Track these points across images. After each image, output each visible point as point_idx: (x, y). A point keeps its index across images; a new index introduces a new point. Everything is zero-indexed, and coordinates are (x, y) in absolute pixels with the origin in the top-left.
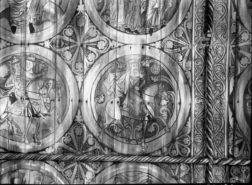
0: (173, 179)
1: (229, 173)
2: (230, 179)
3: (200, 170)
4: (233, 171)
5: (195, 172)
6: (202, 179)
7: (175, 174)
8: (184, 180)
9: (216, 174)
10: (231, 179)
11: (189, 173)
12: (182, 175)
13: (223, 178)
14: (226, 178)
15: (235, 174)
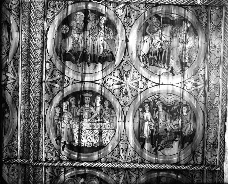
0: (7, 10)
1: (46, 6)
2: (47, 9)
3: (27, 4)
4: (49, 4)
5: (23, 6)
6: (28, 10)
7: (8, 7)
8: (15, 11)
9: (38, 7)
10: (48, 10)
11: (18, 6)
12: (13, 7)
13: (42, 9)
14: (45, 9)
15: (51, 7)
